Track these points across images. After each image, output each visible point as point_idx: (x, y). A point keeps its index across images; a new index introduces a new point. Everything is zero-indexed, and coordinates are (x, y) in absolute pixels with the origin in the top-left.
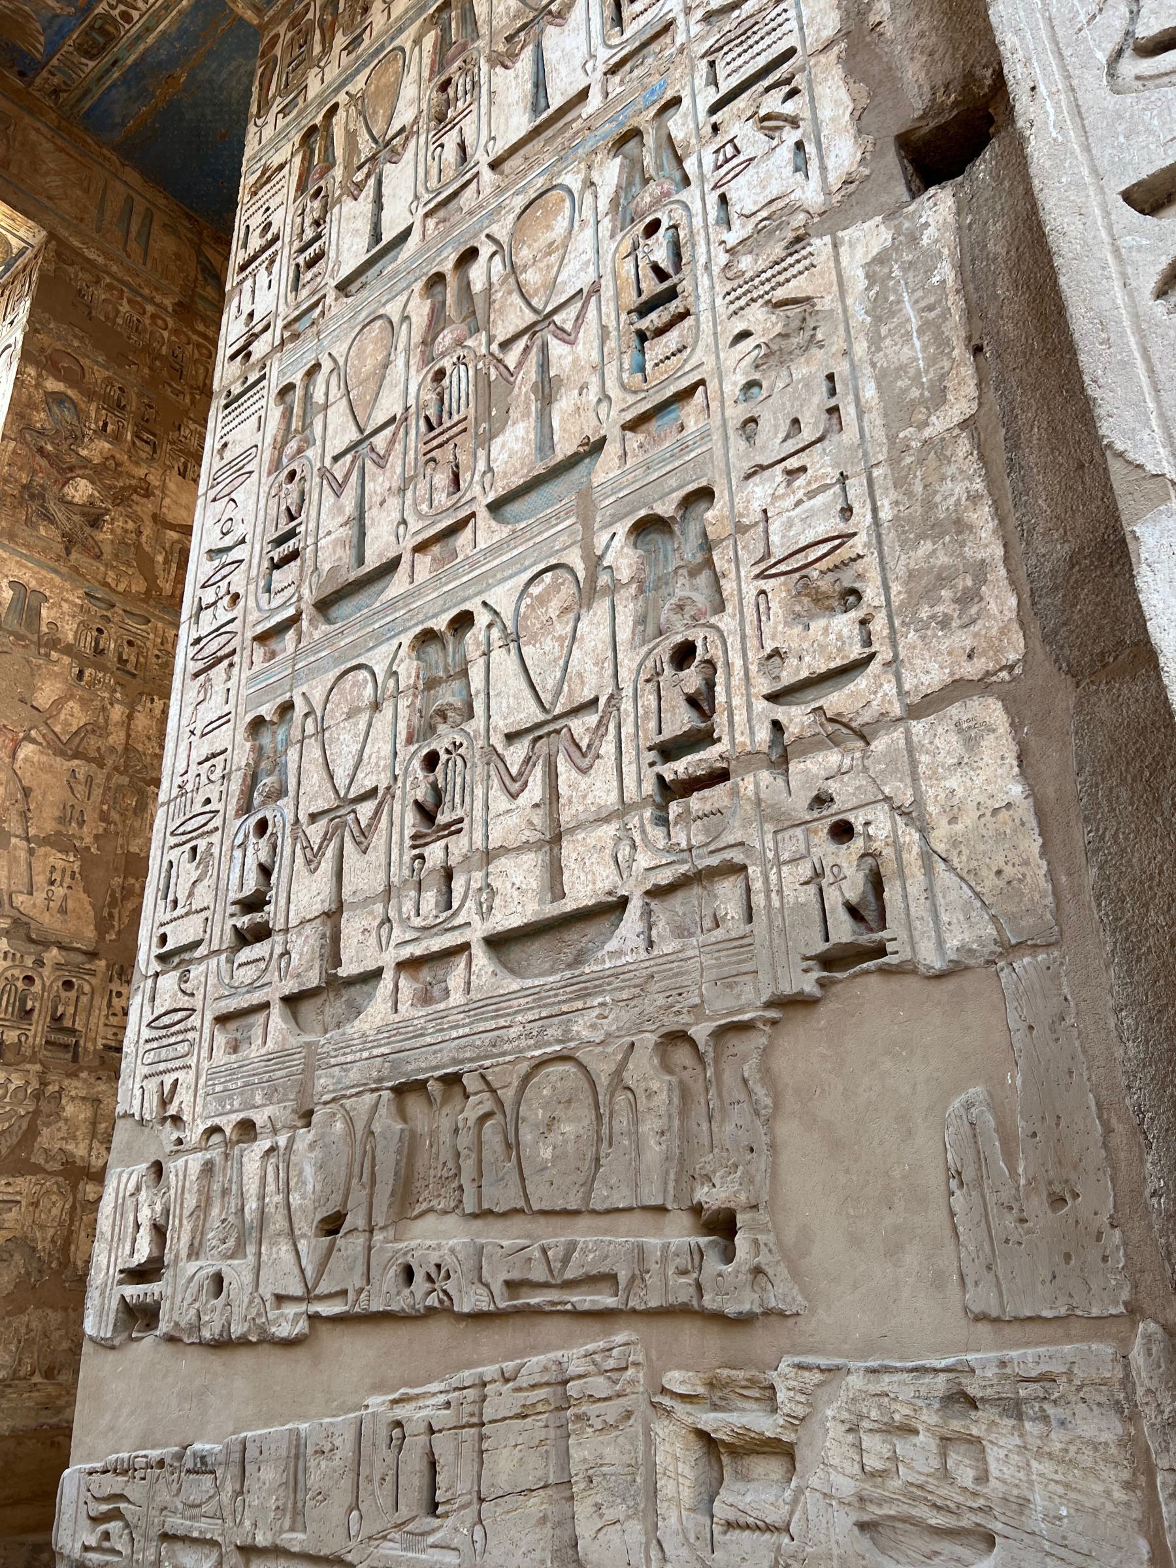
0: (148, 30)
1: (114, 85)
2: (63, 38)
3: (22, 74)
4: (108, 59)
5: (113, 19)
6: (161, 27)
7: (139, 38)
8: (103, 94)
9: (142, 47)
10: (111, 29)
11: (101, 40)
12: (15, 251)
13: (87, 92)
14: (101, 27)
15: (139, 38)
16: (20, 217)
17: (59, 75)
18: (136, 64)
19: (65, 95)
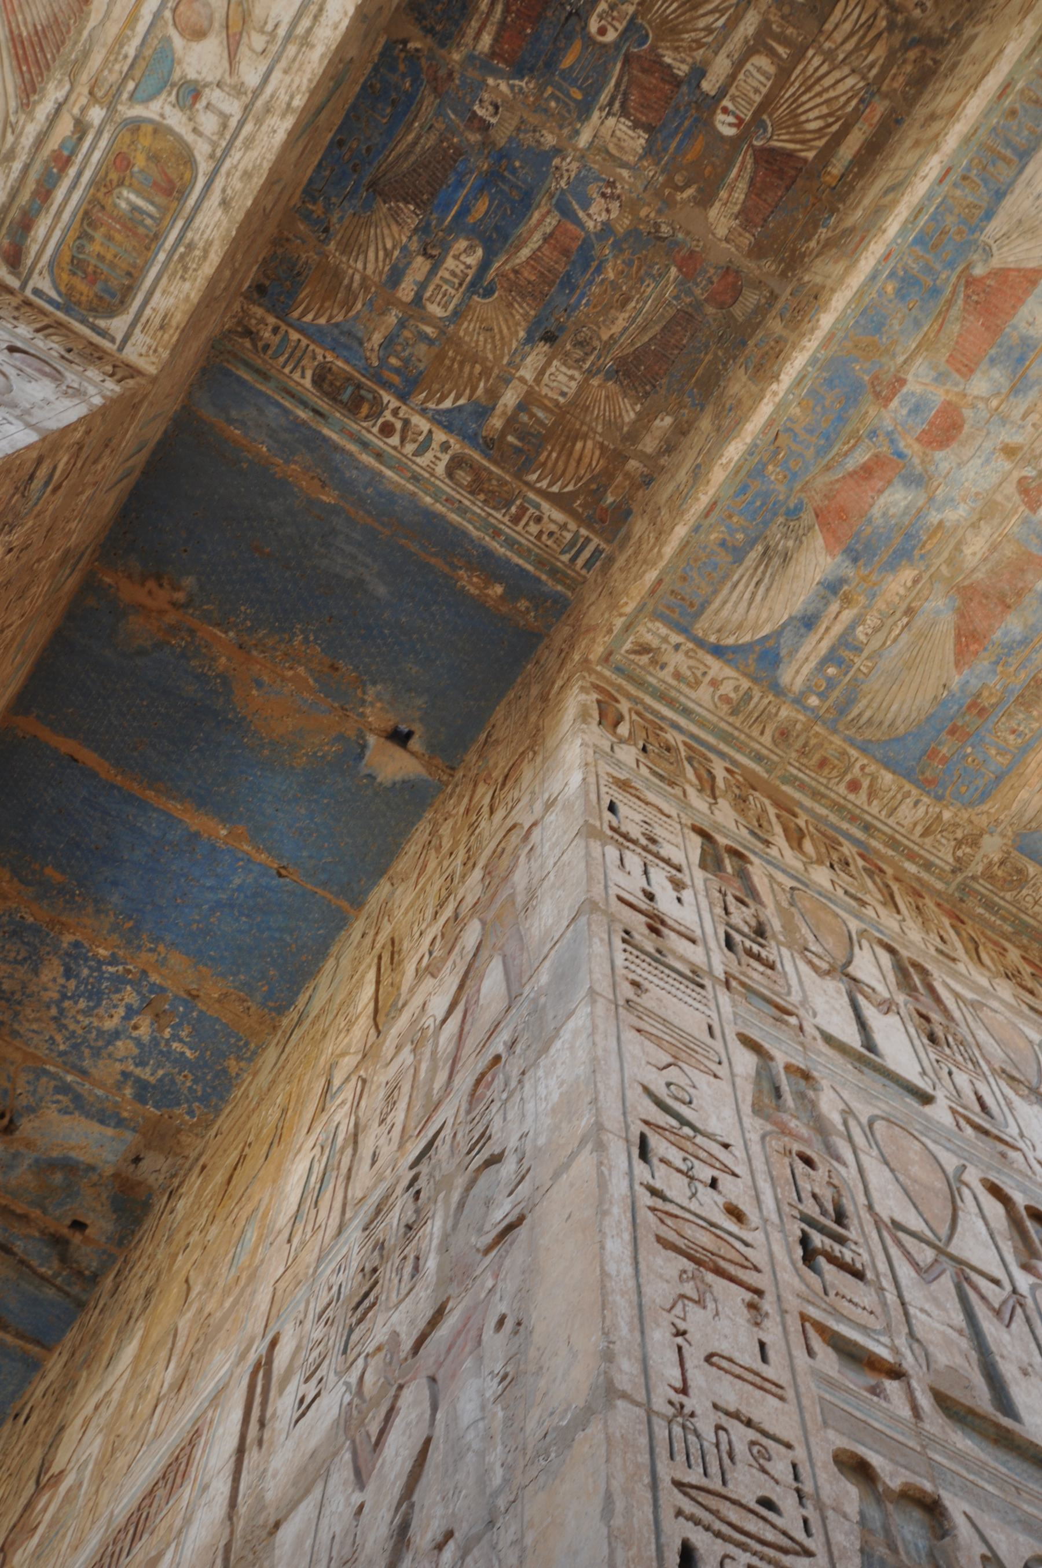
0: (379, 455)
1: (286, 411)
2: (333, 350)
3: (260, 289)
4: (323, 405)
5: (380, 414)
6: (388, 473)
7: (365, 445)
8: (269, 397)
9: (352, 448)
10: (365, 410)
11: (345, 397)
12: (102, 323)
13: (266, 377)
14: (362, 399)
15: (365, 445)
16: (171, 336)
17: (277, 339)
18: (326, 439)
19: (248, 345)
